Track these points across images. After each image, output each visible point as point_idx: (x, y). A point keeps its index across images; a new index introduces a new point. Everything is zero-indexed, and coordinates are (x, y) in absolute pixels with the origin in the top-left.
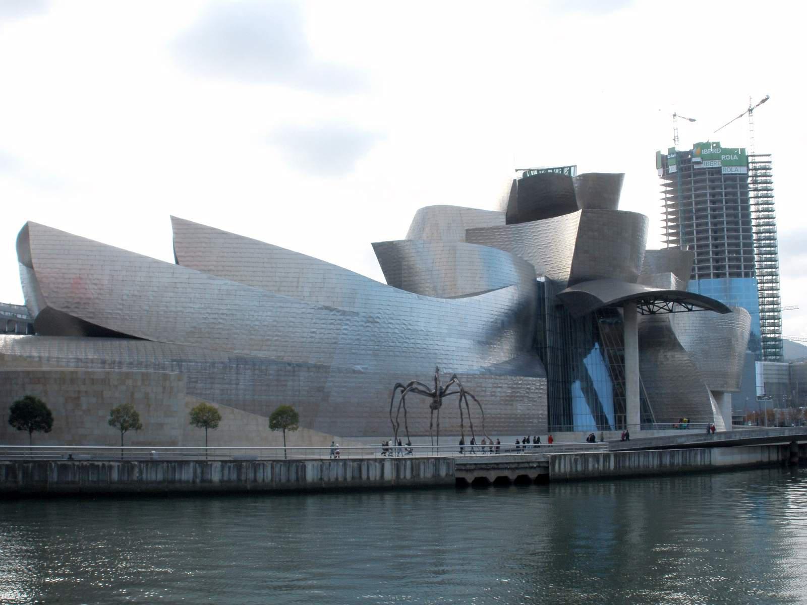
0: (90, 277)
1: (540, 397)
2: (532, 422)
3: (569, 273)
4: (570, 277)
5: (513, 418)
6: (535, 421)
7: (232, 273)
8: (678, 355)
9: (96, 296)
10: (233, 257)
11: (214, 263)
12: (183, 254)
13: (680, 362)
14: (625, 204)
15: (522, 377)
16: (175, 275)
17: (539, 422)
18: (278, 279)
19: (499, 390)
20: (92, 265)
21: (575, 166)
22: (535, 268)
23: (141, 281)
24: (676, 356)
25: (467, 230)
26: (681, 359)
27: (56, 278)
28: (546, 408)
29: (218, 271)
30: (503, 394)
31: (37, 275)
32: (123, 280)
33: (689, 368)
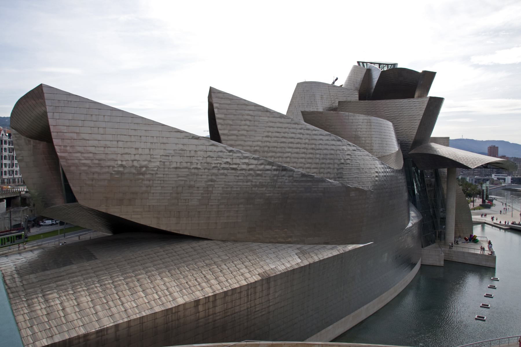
0: (136, 164)
3: (413, 138)
7: (278, 155)
9: (144, 189)
10: (277, 137)
11: (259, 143)
12: (226, 132)
14: (433, 92)
16: (235, 161)
18: (318, 161)
20: (137, 149)
21: (397, 64)
23: (196, 168)
25: (339, 102)
27: (90, 167)
29: (264, 152)
31: (62, 162)
32: (176, 168)
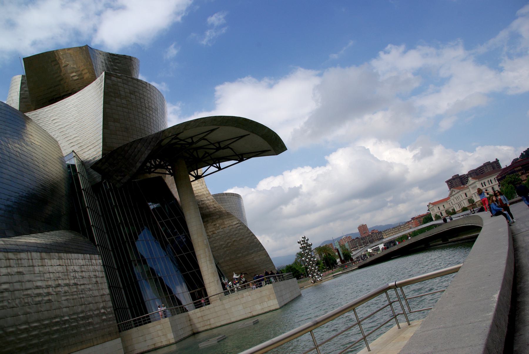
1: (97, 282)
2: (90, 324)
4: (103, 154)
5: (57, 323)
6: (96, 320)
8: (227, 222)
13: (231, 227)
15: (62, 255)
17: (104, 320)
19: (17, 278)
22: (59, 142)
24: (226, 223)
26: (231, 224)
28: (108, 298)
30: (28, 285)
33: (241, 231)
